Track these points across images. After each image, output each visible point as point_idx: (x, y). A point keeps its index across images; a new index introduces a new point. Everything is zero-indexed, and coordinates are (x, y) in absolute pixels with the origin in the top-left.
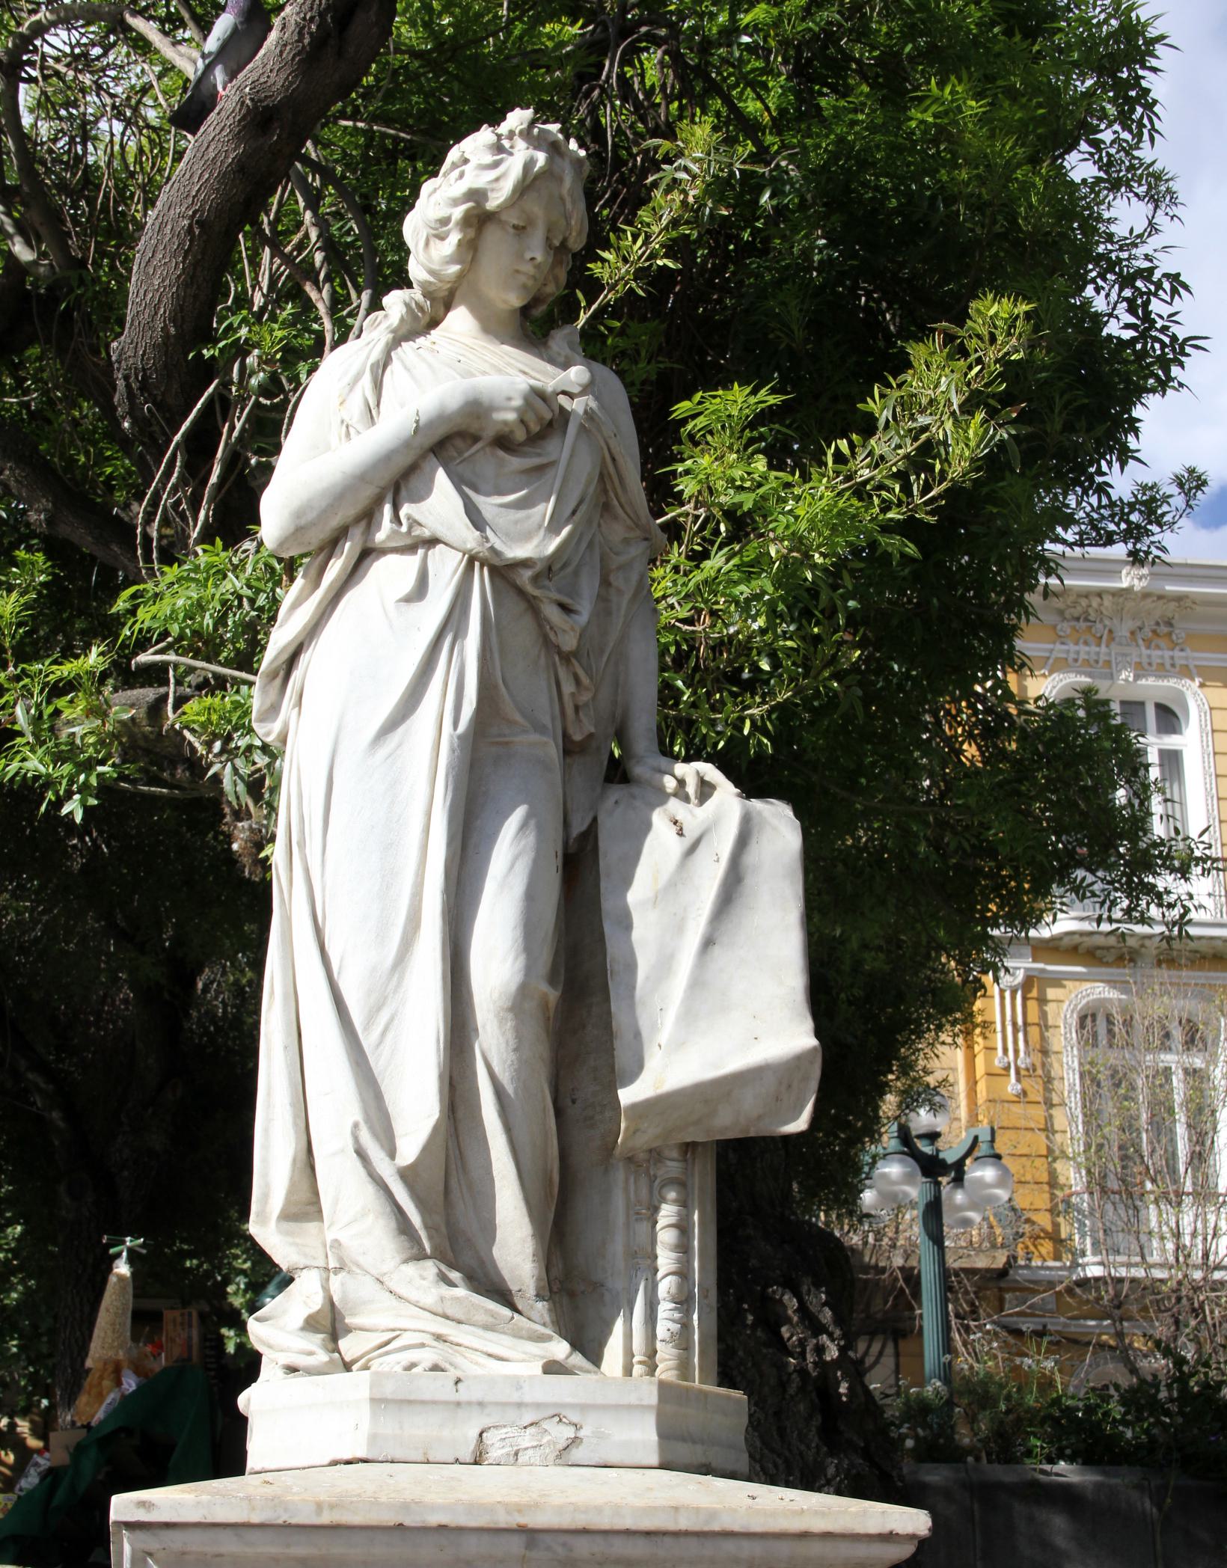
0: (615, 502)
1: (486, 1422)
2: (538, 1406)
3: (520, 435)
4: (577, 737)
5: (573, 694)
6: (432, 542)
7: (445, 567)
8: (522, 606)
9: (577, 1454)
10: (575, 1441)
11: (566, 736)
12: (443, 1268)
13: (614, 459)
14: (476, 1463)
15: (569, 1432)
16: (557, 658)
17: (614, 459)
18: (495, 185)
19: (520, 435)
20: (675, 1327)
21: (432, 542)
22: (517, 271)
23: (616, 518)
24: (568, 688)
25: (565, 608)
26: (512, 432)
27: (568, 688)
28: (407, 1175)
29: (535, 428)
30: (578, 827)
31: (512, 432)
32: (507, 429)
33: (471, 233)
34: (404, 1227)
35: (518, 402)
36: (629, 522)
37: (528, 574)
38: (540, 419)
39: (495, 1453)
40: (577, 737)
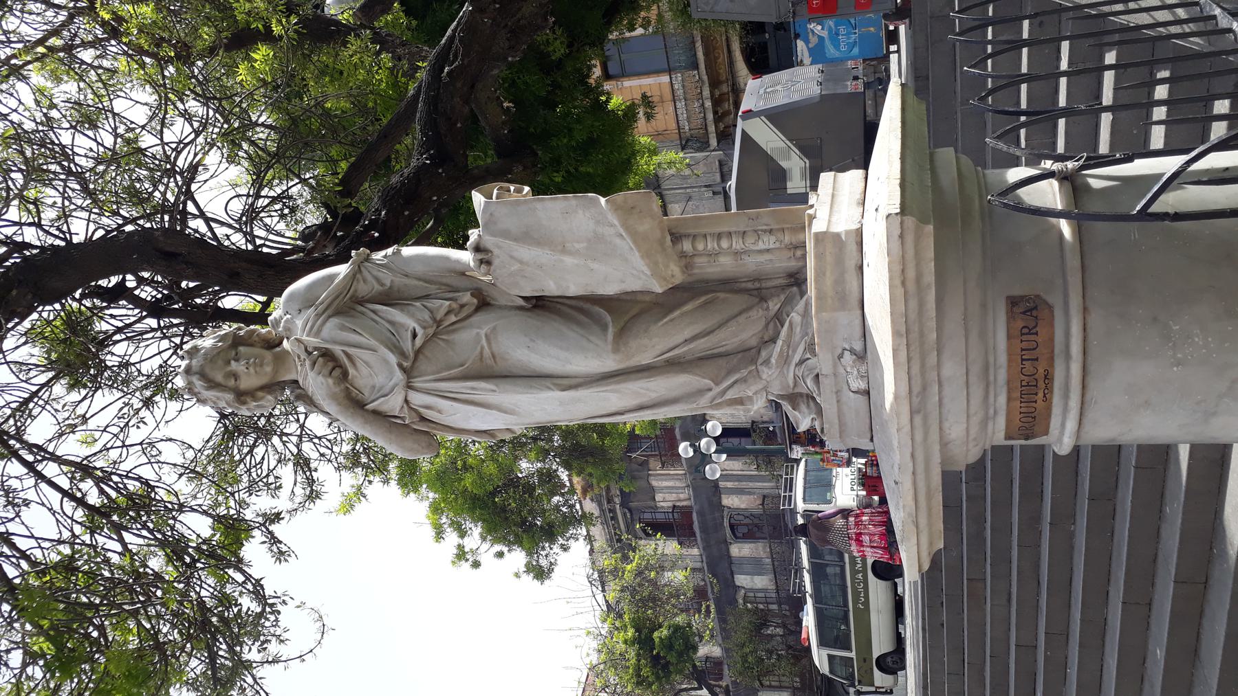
1: (845, 387)
2: (835, 366)
3: (337, 372)
4: (475, 301)
6: (406, 401)
7: (417, 399)
8: (421, 356)
9: (858, 346)
10: (852, 351)
11: (478, 309)
12: (760, 361)
14: (868, 393)
15: (847, 354)
19: (337, 372)
20: (773, 239)
21: (406, 401)
25: (415, 335)
27: (453, 318)
28: (717, 384)
29: (331, 365)
30: (521, 302)
34: (744, 380)
35: (320, 378)
37: (405, 364)
38: (325, 364)
39: (862, 385)
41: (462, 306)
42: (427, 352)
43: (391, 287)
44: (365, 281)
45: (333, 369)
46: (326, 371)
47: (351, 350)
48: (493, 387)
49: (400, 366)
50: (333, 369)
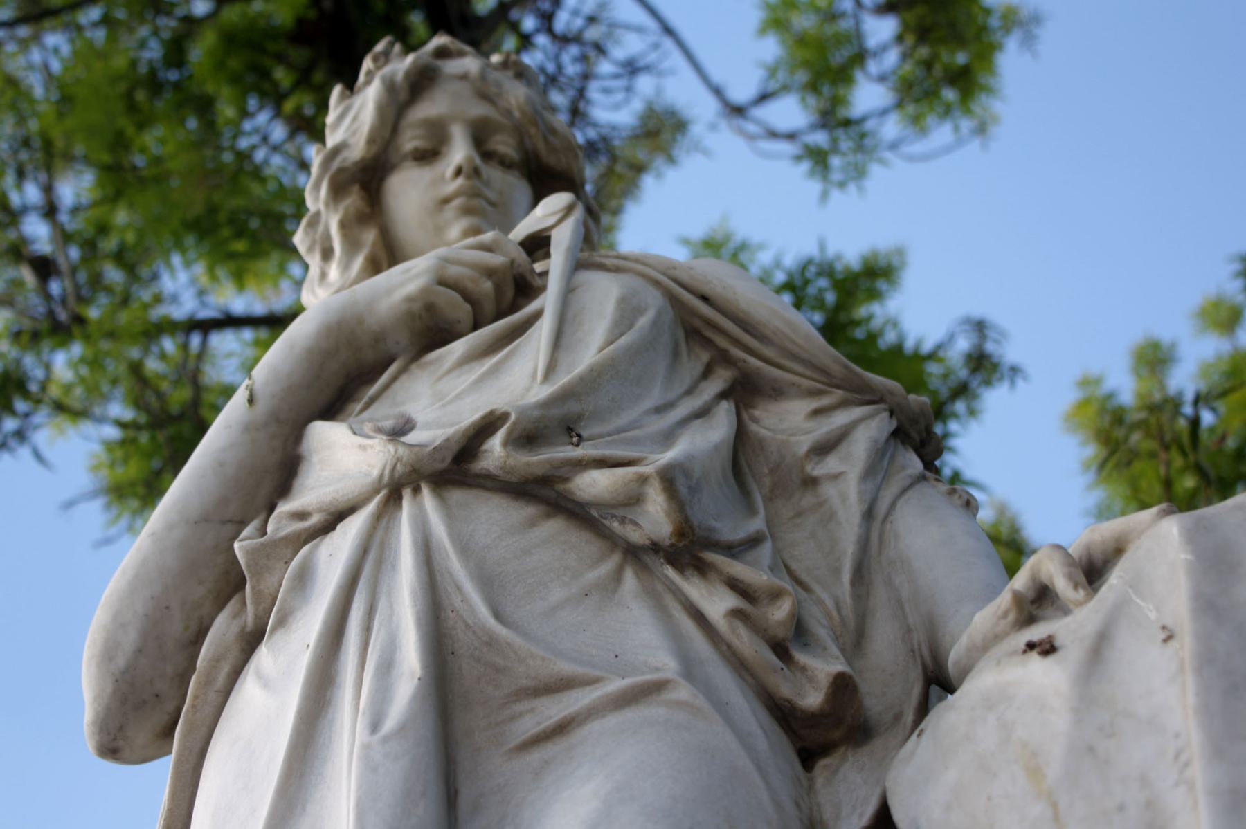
0: (754, 362)
4: (813, 699)
5: (736, 614)
11: (783, 714)
13: (705, 299)
16: (670, 572)
17: (705, 299)
18: (355, 126)
22: (446, 201)
23: (777, 392)
24: (718, 604)
26: (430, 308)
31: (430, 308)
32: (417, 306)
33: (354, 200)
36: (806, 383)
38: (490, 273)
40: (813, 699)
41: (781, 650)
42: (555, 526)
43: (811, 482)
44: (817, 413)
45: (467, 297)
46: (453, 271)
47: (543, 331)
48: (391, 722)
49: (487, 426)
50: (467, 297)
